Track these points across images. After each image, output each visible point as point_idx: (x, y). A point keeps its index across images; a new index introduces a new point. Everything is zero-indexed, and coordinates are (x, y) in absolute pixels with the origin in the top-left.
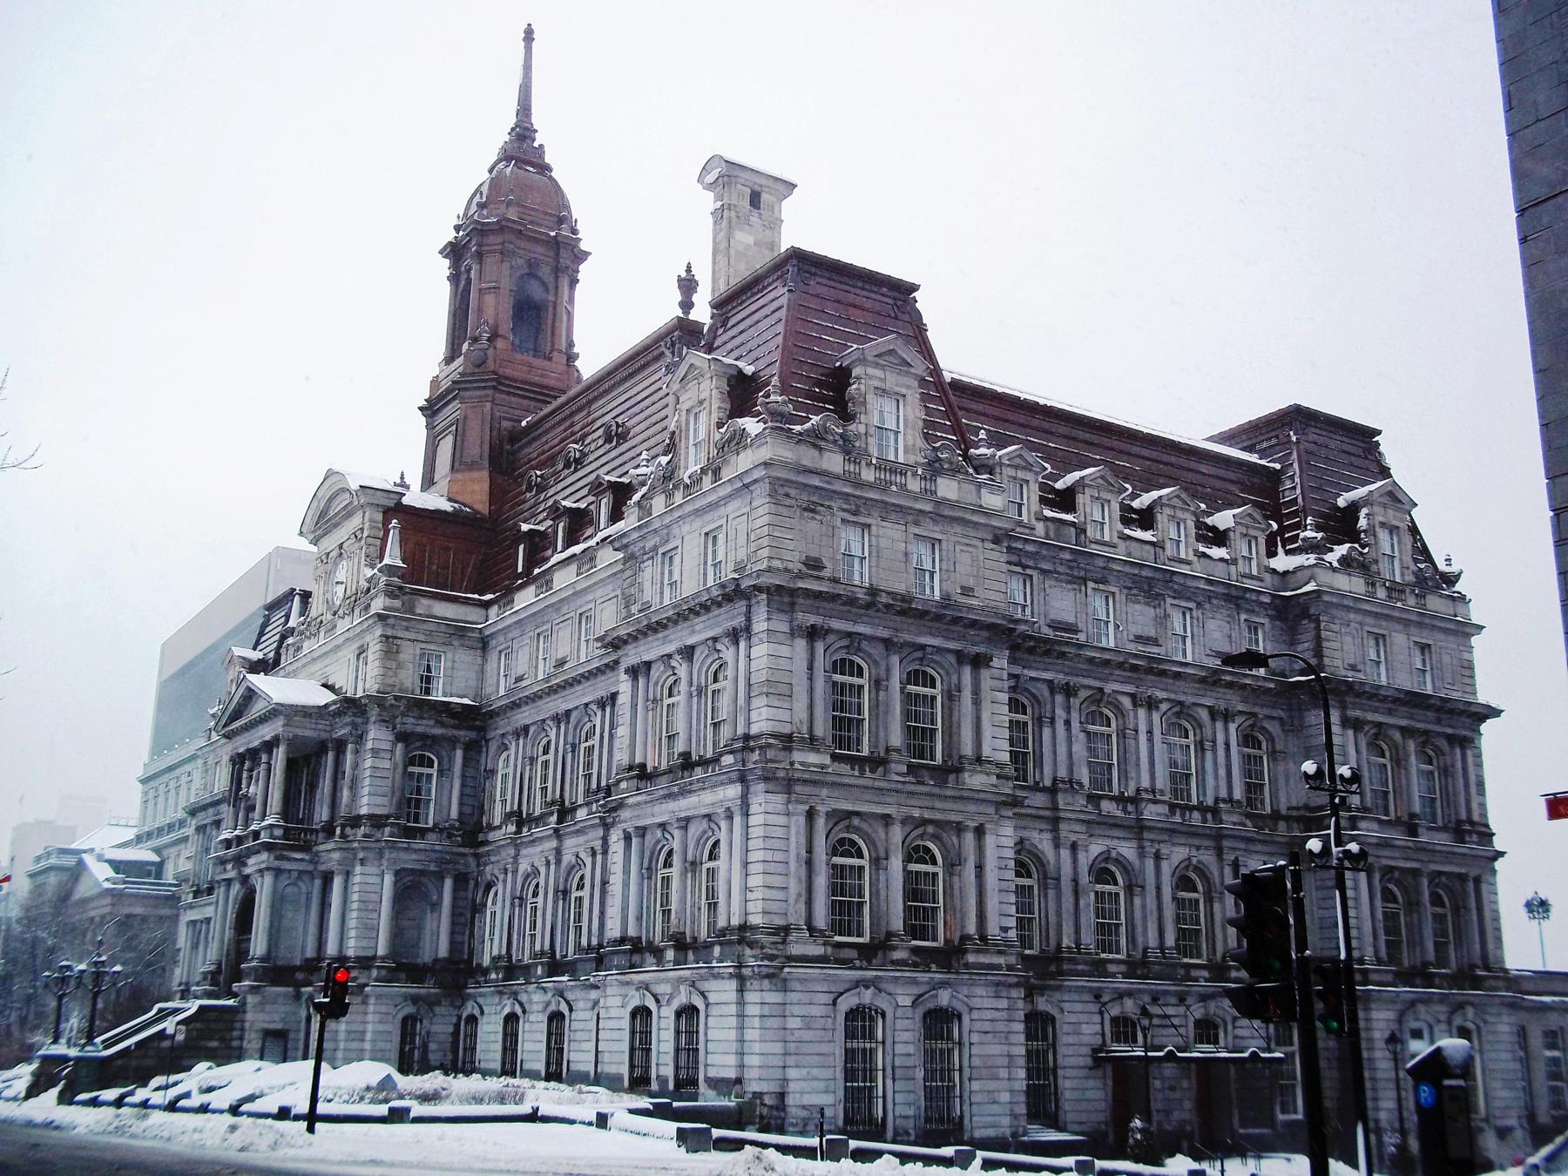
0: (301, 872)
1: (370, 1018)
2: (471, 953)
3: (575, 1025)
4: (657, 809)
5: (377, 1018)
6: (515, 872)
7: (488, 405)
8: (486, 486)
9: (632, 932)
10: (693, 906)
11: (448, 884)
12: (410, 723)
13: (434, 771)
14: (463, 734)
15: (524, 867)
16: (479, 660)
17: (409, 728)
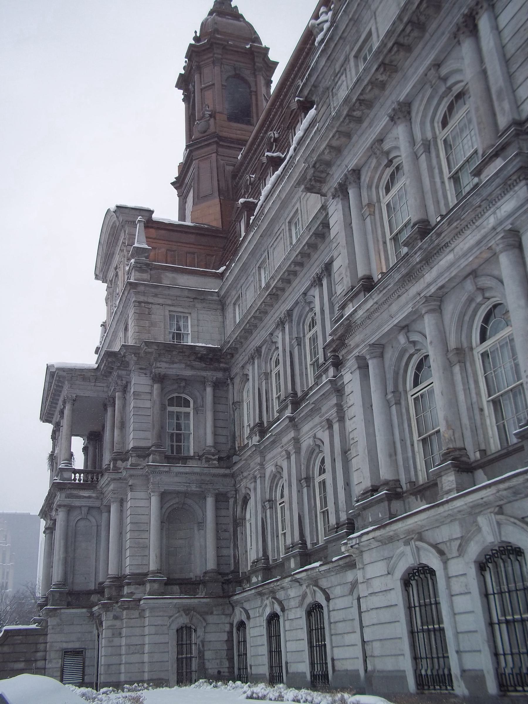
0: (90, 508)
1: (147, 630)
2: (237, 563)
3: (336, 616)
4: (394, 308)
5: (153, 630)
6: (263, 477)
7: (214, 155)
8: (218, 208)
9: (385, 474)
10: (470, 408)
11: (210, 502)
12: (163, 367)
13: (190, 410)
14: (210, 375)
15: (270, 469)
16: (220, 319)
17: (163, 371)
